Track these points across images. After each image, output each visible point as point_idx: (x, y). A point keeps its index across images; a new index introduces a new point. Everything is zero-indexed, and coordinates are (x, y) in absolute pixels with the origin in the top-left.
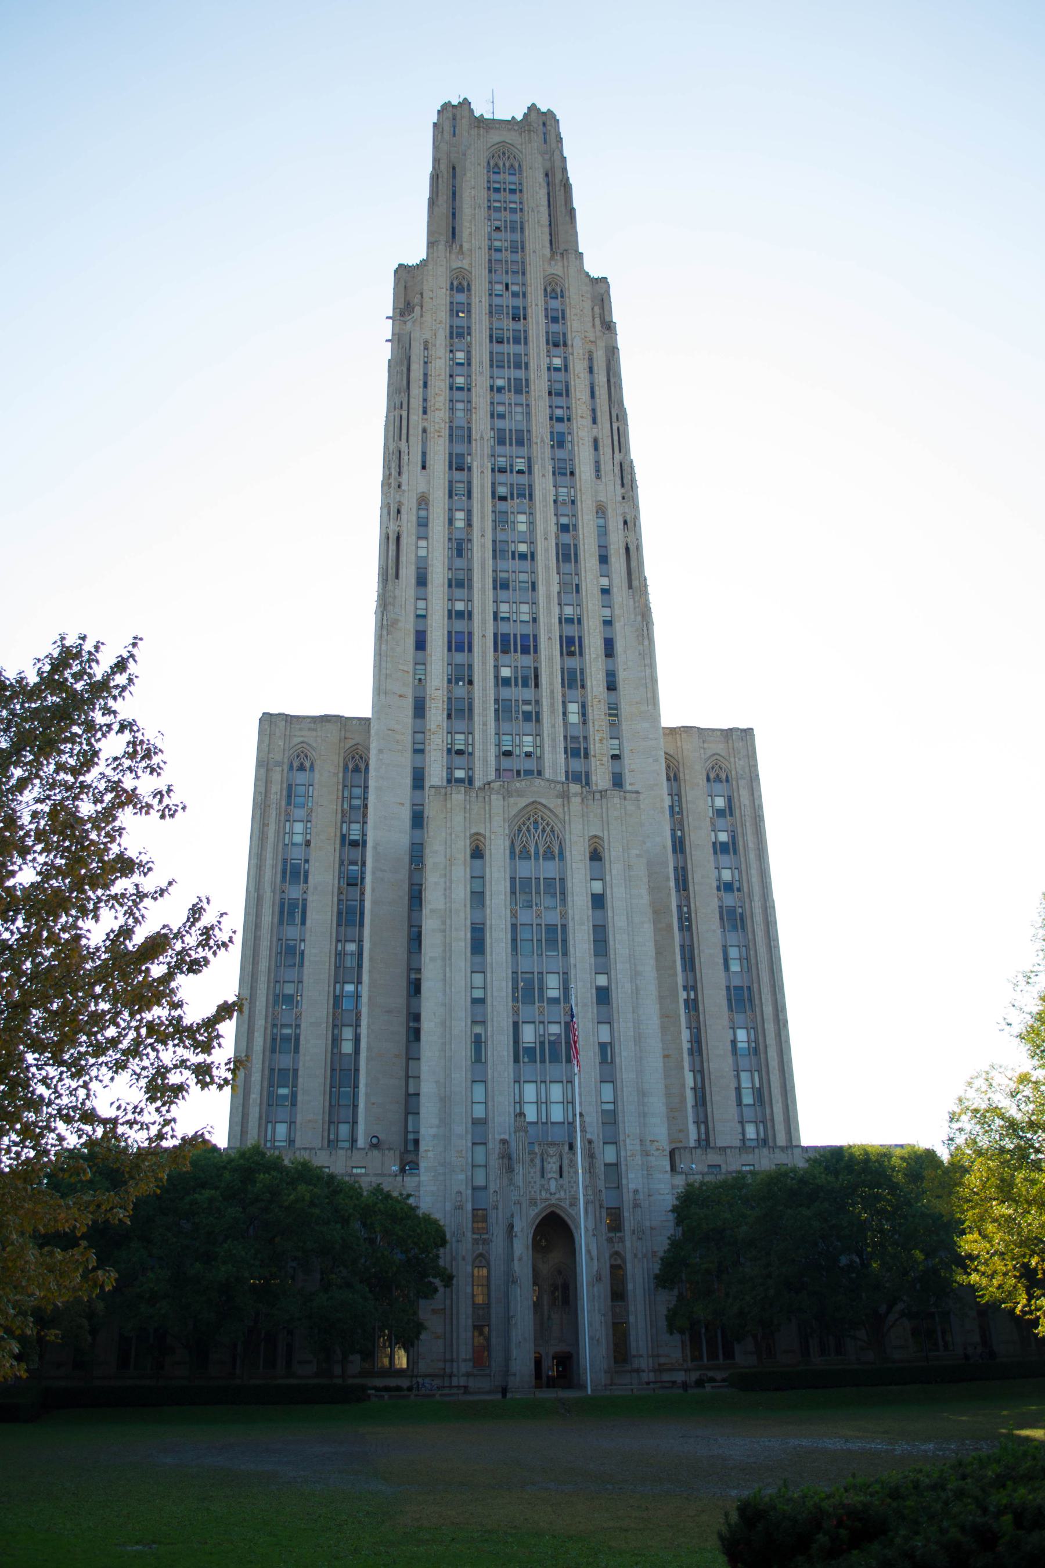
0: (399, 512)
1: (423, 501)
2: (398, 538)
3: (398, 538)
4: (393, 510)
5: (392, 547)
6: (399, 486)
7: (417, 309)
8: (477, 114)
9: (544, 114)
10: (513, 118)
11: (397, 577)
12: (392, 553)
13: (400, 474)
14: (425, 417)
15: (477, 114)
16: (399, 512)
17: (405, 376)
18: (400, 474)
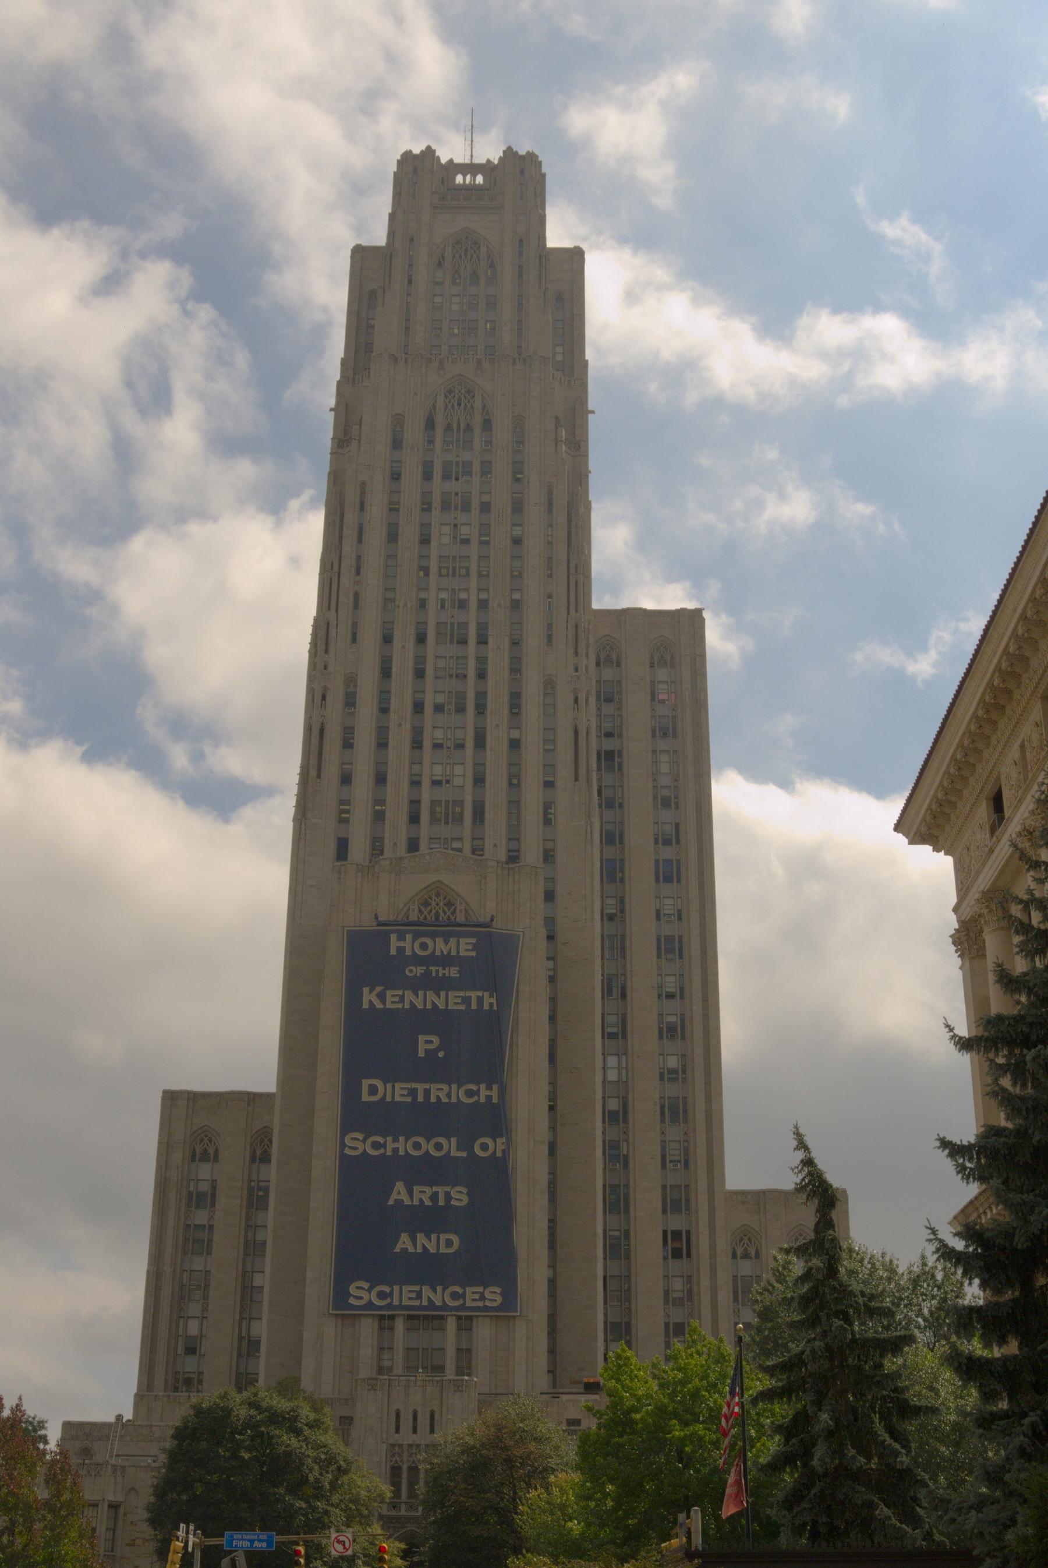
0: (324, 698)
1: (351, 680)
2: (322, 731)
3: (322, 731)
4: (318, 697)
5: (315, 741)
6: (325, 668)
7: (354, 443)
8: (444, 161)
9: (522, 157)
10: (488, 161)
11: (319, 776)
12: (315, 748)
13: (326, 652)
14: (358, 578)
15: (443, 161)
16: (324, 698)
17: (337, 528)
18: (326, 652)
